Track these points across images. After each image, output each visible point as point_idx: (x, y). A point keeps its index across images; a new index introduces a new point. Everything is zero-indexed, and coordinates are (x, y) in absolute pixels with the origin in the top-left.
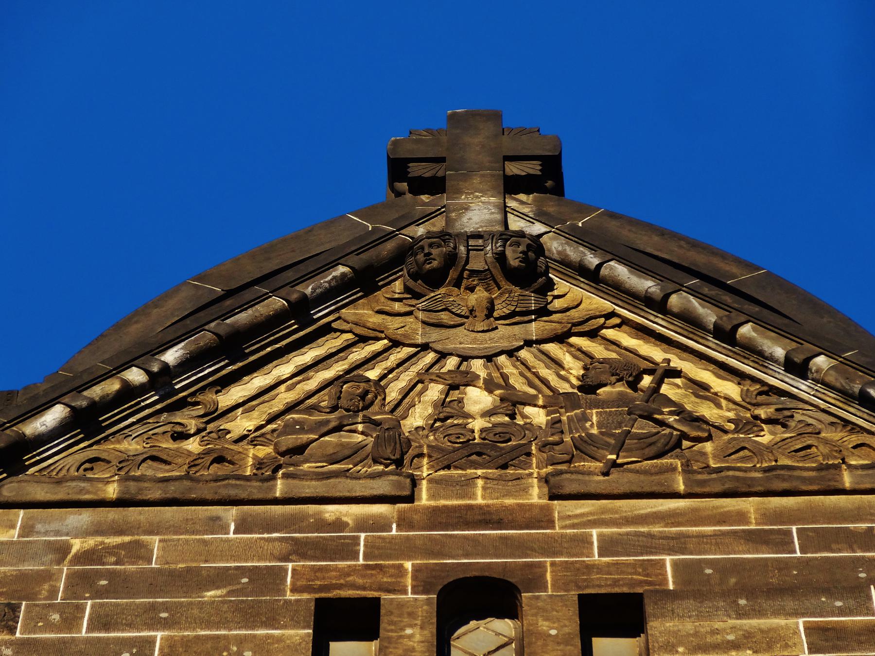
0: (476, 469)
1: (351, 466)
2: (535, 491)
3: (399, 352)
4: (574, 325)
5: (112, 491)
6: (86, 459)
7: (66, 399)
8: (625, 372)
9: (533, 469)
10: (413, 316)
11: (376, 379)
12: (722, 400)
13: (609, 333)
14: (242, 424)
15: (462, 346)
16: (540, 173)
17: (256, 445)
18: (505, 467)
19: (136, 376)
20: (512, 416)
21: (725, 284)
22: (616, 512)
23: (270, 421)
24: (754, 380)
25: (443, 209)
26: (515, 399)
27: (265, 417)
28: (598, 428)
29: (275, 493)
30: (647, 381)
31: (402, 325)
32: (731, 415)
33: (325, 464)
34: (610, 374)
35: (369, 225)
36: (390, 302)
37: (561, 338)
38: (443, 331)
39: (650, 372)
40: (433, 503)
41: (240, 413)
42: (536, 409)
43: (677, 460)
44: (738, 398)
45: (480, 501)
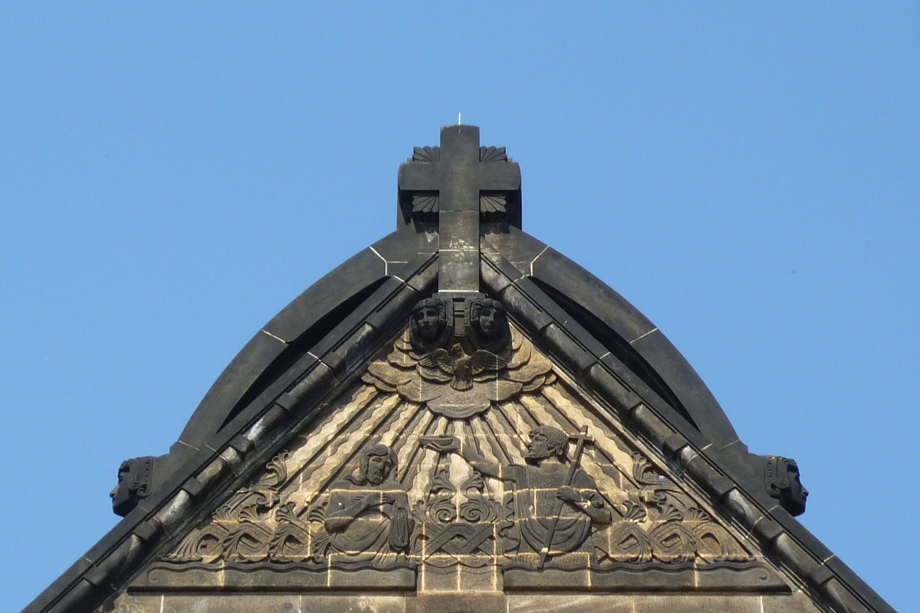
0: (457, 554)
1: (375, 553)
2: (495, 580)
3: (407, 409)
4: (525, 384)
5: (220, 579)
6: (202, 536)
7: (186, 486)
8: (557, 447)
9: (494, 554)
10: (416, 371)
11: (390, 444)
12: (620, 474)
13: (549, 391)
14: (302, 495)
15: (449, 405)
16: (505, 211)
17: (312, 521)
18: (476, 550)
19: (230, 455)
20: (481, 490)
21: (629, 344)
22: (547, 607)
23: (322, 491)
24: (643, 455)
25: (437, 254)
26: (484, 470)
27: (318, 487)
28: (538, 515)
29: (327, 583)
30: (572, 448)
31: (408, 379)
32: (624, 494)
33: (357, 552)
34: (547, 448)
35: (385, 261)
36: (400, 353)
37: (515, 398)
38: (436, 387)
39: (574, 441)
40: (428, 592)
41: (301, 481)
42: (497, 481)
43: (587, 553)
44: (630, 473)
45: (459, 591)
